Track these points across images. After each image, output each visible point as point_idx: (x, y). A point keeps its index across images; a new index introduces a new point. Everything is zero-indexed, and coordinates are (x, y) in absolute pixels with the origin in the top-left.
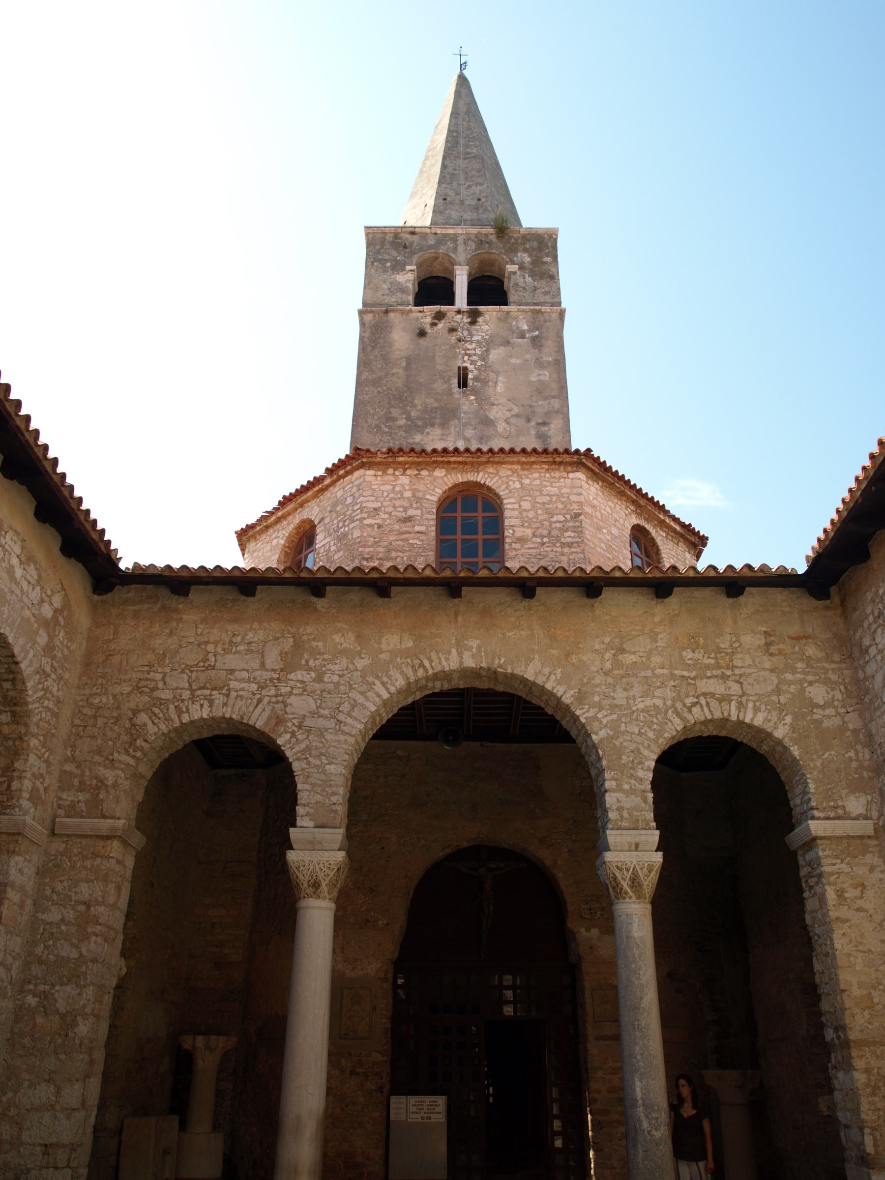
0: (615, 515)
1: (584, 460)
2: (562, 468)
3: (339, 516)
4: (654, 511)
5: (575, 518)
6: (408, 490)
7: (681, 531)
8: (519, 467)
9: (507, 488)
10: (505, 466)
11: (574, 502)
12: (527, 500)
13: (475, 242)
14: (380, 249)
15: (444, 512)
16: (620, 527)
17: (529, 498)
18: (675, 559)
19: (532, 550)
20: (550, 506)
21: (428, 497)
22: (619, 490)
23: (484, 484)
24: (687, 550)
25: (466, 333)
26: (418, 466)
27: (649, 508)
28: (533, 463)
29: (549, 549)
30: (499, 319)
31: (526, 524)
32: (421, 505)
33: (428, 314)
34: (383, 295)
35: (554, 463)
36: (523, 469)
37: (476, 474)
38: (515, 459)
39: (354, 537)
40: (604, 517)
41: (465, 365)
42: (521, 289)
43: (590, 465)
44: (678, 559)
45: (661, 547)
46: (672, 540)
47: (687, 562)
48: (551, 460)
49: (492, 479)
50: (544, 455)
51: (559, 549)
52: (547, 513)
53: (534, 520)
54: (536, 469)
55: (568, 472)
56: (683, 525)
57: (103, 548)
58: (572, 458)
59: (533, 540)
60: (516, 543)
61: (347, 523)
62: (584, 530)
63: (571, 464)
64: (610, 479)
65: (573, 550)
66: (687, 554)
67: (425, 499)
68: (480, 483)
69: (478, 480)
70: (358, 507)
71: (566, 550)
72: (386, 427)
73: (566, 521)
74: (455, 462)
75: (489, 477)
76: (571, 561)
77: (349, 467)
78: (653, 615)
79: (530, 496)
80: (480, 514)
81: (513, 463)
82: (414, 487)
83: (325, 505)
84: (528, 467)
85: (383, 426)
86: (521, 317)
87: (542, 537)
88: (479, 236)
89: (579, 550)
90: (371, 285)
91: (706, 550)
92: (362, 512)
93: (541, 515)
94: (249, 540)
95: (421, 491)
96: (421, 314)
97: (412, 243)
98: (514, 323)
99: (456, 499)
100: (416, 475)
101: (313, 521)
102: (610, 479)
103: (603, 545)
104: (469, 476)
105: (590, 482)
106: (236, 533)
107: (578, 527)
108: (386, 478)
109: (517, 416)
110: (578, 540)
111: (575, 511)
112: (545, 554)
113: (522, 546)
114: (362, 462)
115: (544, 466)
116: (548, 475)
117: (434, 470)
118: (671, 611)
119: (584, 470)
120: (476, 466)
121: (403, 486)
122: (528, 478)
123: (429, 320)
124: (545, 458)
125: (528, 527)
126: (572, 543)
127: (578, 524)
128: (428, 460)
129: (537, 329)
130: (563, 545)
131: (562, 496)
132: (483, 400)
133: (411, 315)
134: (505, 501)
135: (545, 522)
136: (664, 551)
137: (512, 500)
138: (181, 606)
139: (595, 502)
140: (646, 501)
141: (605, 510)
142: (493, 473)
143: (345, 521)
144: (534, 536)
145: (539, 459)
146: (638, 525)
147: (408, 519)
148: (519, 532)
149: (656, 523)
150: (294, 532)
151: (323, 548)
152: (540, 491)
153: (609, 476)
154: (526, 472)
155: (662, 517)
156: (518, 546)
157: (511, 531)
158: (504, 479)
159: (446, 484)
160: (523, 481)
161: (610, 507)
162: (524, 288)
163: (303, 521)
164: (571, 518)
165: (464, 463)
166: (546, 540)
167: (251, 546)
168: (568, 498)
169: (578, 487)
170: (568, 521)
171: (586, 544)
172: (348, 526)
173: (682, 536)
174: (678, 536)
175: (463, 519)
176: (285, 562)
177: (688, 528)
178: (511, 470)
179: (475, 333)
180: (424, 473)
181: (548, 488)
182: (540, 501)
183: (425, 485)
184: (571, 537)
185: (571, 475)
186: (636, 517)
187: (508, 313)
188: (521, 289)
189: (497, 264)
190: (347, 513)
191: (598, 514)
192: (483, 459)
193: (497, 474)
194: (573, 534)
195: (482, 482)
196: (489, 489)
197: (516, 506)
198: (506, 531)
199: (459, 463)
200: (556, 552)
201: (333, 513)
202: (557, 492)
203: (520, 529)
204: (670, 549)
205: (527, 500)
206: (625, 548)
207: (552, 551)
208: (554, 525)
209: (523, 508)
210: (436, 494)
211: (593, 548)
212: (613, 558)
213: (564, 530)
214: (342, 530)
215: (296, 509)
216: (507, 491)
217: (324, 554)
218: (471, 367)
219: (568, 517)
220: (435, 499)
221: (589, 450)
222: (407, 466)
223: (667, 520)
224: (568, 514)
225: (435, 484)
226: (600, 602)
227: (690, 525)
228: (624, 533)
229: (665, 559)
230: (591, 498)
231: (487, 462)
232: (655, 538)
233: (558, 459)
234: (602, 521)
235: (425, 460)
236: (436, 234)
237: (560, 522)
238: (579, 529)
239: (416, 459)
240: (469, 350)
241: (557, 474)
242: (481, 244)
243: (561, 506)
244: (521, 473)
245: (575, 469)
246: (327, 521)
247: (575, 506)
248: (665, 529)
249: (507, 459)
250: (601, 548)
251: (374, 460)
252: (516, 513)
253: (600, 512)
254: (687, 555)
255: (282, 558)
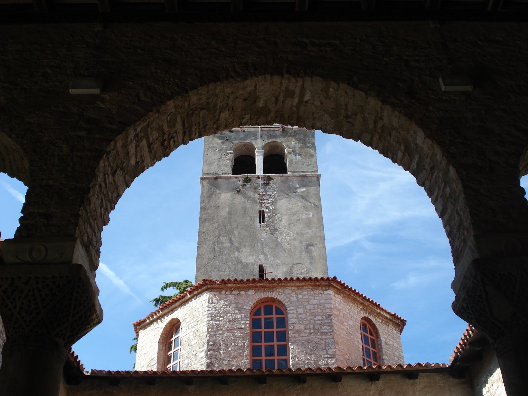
0: (351, 313)
1: (332, 283)
2: (320, 288)
3: (194, 318)
4: (373, 307)
5: (328, 317)
6: (233, 303)
7: (390, 318)
8: (296, 288)
9: (289, 301)
10: (288, 288)
11: (327, 308)
12: (301, 308)
13: (267, 136)
14: (212, 141)
15: (254, 315)
16: (354, 320)
17: (302, 307)
18: (387, 335)
19: (305, 337)
20: (314, 311)
21: (245, 307)
22: (353, 298)
23: (277, 298)
24: (394, 328)
25: (263, 190)
26: (239, 289)
27: (371, 306)
28: (303, 286)
29: (314, 337)
30: (282, 181)
31: (301, 322)
32: (241, 312)
33: (241, 179)
34: (214, 168)
35: (315, 285)
36: (298, 289)
37: (272, 292)
38: (293, 284)
39: (203, 332)
40: (345, 315)
41: (263, 209)
42: (294, 163)
43: (336, 286)
44: (389, 335)
45: (379, 329)
46: (385, 324)
47: (394, 336)
48: (314, 284)
49: (281, 295)
50: (309, 281)
51: (320, 337)
52: (312, 315)
53: (305, 319)
54: (305, 289)
55: (324, 291)
56: (391, 315)
57: (76, 365)
58: (326, 282)
59: (304, 332)
60: (295, 333)
61: (199, 323)
62: (333, 324)
63: (325, 286)
64: (347, 292)
65: (328, 337)
66: (394, 331)
67: (243, 308)
68: (274, 298)
69: (273, 297)
70: (206, 313)
71: (324, 337)
72: (218, 247)
73: (323, 319)
74: (259, 286)
75: (279, 294)
76: (327, 344)
77: (200, 290)
78: (370, 391)
79: (302, 305)
80: (274, 316)
81: (292, 286)
82: (237, 301)
83: (186, 311)
84: (301, 288)
85: (216, 247)
86: (295, 180)
87: (310, 329)
88: (269, 132)
89: (331, 337)
90: (207, 163)
91: (405, 327)
92: (208, 317)
93: (309, 316)
94: (141, 329)
95: (241, 304)
96: (237, 179)
97: (230, 137)
98: (291, 184)
99: (260, 308)
100: (238, 294)
101: (179, 320)
102: (347, 292)
103: (345, 332)
104: (268, 294)
105: (336, 295)
106: (133, 324)
107: (330, 323)
108: (221, 296)
109: (295, 239)
110: (330, 331)
111: (327, 314)
112: (312, 339)
113: (299, 335)
114: (207, 287)
115: (310, 287)
116: (312, 292)
117: (248, 291)
118: (379, 388)
119: (332, 288)
120: (271, 289)
121: (230, 300)
122: (301, 295)
123: (241, 182)
124: (310, 283)
125: (302, 324)
126: (327, 333)
127: (330, 321)
128: (245, 285)
129: (304, 186)
130: (322, 334)
131: (320, 304)
132: (273, 231)
133: (231, 180)
134: (288, 309)
135: (311, 321)
136: (381, 331)
137: (292, 308)
138: (115, 391)
139: (339, 307)
140: (368, 303)
141: (345, 311)
142: (281, 292)
143: (198, 322)
144: (305, 329)
145: (307, 283)
146: (365, 317)
147: (234, 321)
148: (297, 327)
149: (375, 314)
150: (168, 325)
151: (185, 337)
152: (308, 302)
153: (346, 291)
154: (300, 291)
155: (378, 311)
156: (296, 335)
157: (292, 327)
158: (287, 295)
159: (255, 299)
160: (298, 296)
161: (348, 309)
162: (296, 163)
163: (173, 319)
164: (326, 318)
165: (265, 287)
166: (312, 331)
167: (142, 332)
168: (324, 306)
169: (330, 299)
170: (325, 320)
171: (335, 333)
172: (200, 324)
173: (391, 320)
174: (389, 321)
175: (265, 319)
176: (163, 343)
177: (394, 316)
178: (291, 290)
179: (268, 190)
180: (243, 293)
181: (313, 300)
182: (308, 308)
183: (243, 300)
184: (326, 329)
185: (325, 292)
186: (364, 313)
187: (287, 177)
188: (294, 163)
189: (280, 148)
190: (199, 317)
191: (341, 314)
192: (276, 284)
193: (284, 292)
194: (327, 328)
195: (275, 298)
196: (279, 301)
197: (295, 311)
198: (289, 327)
199: (262, 287)
200: (318, 338)
201: (191, 316)
202: (318, 303)
203: (298, 325)
204: (384, 329)
205: (301, 308)
206: (358, 332)
207: (316, 337)
208: (316, 322)
209: (299, 312)
210: (249, 305)
211: (339, 335)
212: (351, 340)
213: (322, 325)
214: (196, 326)
215: (169, 312)
216: (289, 303)
217: (187, 340)
218: (266, 211)
219: (324, 317)
220: (249, 308)
221: (335, 278)
222: (232, 289)
223: (382, 313)
224: (324, 315)
225: (249, 299)
226: (341, 384)
227: (395, 314)
228: (356, 323)
229: (381, 336)
230: (337, 305)
231: (277, 286)
232: (375, 324)
233: (318, 283)
234: (344, 318)
235: (243, 285)
236: (244, 131)
237: (320, 320)
238: (331, 324)
239: (237, 285)
240: (265, 200)
241: (317, 292)
242: (271, 136)
243: (320, 311)
244: (297, 291)
245: (327, 288)
246: (187, 320)
247: (328, 311)
248: (380, 317)
249: (289, 284)
250: (344, 334)
251: (214, 286)
252: (295, 316)
253: (343, 313)
254: (395, 332)
255: (161, 341)
